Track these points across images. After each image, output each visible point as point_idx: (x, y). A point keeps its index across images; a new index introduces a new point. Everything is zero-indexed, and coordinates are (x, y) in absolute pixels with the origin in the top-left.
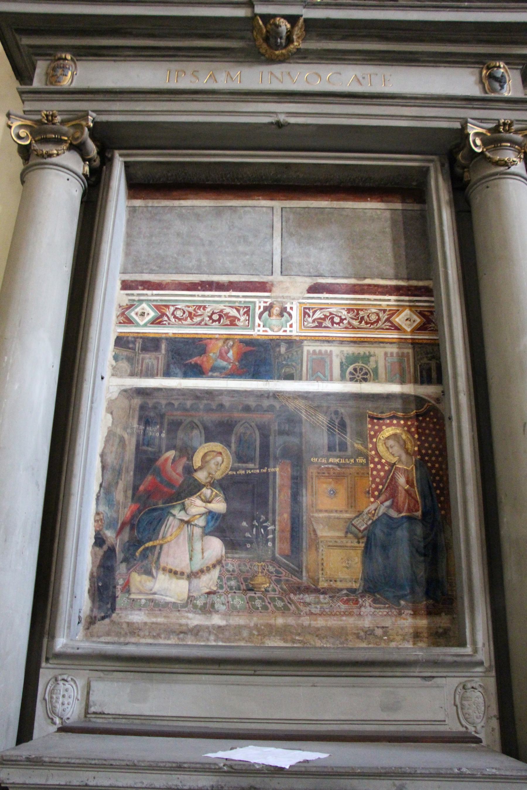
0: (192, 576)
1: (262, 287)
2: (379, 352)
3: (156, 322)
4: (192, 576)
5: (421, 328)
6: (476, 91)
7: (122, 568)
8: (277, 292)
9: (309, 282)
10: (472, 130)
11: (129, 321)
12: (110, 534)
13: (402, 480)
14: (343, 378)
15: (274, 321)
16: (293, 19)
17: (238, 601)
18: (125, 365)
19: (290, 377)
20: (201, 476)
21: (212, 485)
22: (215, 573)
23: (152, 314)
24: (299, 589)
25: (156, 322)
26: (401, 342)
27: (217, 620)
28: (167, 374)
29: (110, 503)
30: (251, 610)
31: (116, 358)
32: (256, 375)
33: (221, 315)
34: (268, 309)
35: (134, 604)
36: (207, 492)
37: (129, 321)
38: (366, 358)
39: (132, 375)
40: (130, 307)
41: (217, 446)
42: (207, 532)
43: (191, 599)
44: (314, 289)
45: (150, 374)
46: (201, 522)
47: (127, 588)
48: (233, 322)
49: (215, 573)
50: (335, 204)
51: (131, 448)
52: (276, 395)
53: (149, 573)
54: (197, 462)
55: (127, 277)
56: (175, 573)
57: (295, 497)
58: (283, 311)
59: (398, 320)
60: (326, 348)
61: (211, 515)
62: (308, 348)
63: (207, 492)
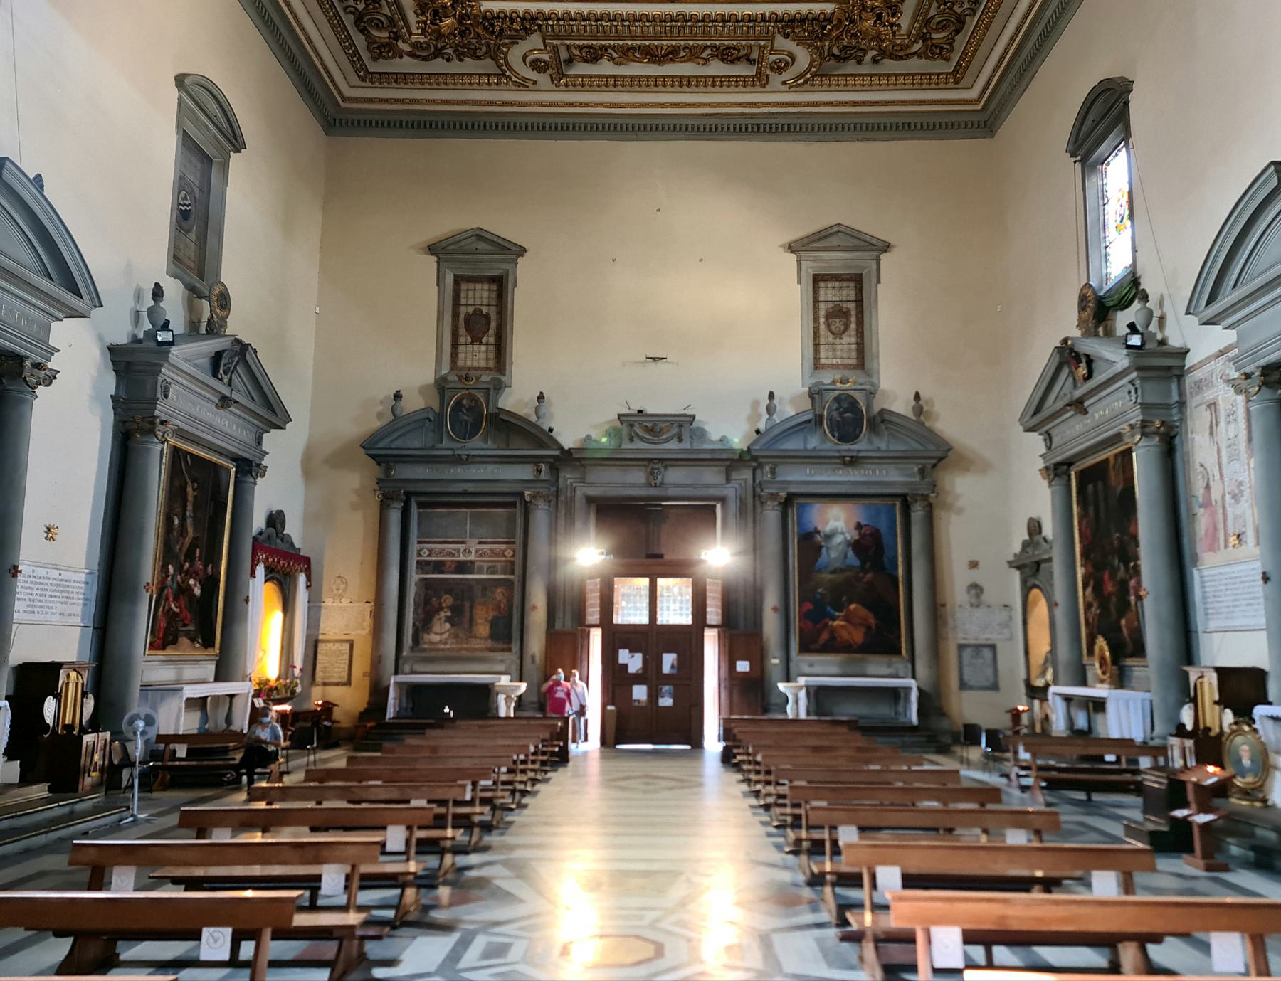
0: (441, 634)
1: (463, 543)
3: (429, 555)
4: (441, 634)
7: (421, 633)
8: (468, 545)
9: (477, 540)
11: (420, 555)
12: (417, 623)
13: (502, 606)
14: (487, 573)
15: (467, 554)
17: (454, 641)
18: (420, 571)
19: (470, 573)
21: (447, 607)
22: (447, 634)
23: (427, 553)
24: (471, 637)
25: (429, 555)
26: (505, 561)
27: (448, 646)
28: (433, 573)
29: (417, 614)
30: (457, 643)
31: (417, 568)
32: (460, 573)
33: (450, 553)
34: (465, 550)
35: (425, 643)
36: (445, 610)
37: (420, 555)
38: (494, 567)
39: (422, 573)
41: (447, 596)
42: (446, 621)
43: (441, 641)
44: (480, 543)
45: (427, 573)
46: (444, 619)
47: (422, 639)
48: (453, 555)
49: (447, 634)
51: (423, 597)
52: (467, 579)
53: (428, 633)
54: (442, 601)
55: (419, 539)
56: (436, 634)
57: (471, 611)
58: (469, 551)
59: (506, 553)
60: (482, 564)
61: (446, 617)
62: (477, 564)
63: (445, 610)
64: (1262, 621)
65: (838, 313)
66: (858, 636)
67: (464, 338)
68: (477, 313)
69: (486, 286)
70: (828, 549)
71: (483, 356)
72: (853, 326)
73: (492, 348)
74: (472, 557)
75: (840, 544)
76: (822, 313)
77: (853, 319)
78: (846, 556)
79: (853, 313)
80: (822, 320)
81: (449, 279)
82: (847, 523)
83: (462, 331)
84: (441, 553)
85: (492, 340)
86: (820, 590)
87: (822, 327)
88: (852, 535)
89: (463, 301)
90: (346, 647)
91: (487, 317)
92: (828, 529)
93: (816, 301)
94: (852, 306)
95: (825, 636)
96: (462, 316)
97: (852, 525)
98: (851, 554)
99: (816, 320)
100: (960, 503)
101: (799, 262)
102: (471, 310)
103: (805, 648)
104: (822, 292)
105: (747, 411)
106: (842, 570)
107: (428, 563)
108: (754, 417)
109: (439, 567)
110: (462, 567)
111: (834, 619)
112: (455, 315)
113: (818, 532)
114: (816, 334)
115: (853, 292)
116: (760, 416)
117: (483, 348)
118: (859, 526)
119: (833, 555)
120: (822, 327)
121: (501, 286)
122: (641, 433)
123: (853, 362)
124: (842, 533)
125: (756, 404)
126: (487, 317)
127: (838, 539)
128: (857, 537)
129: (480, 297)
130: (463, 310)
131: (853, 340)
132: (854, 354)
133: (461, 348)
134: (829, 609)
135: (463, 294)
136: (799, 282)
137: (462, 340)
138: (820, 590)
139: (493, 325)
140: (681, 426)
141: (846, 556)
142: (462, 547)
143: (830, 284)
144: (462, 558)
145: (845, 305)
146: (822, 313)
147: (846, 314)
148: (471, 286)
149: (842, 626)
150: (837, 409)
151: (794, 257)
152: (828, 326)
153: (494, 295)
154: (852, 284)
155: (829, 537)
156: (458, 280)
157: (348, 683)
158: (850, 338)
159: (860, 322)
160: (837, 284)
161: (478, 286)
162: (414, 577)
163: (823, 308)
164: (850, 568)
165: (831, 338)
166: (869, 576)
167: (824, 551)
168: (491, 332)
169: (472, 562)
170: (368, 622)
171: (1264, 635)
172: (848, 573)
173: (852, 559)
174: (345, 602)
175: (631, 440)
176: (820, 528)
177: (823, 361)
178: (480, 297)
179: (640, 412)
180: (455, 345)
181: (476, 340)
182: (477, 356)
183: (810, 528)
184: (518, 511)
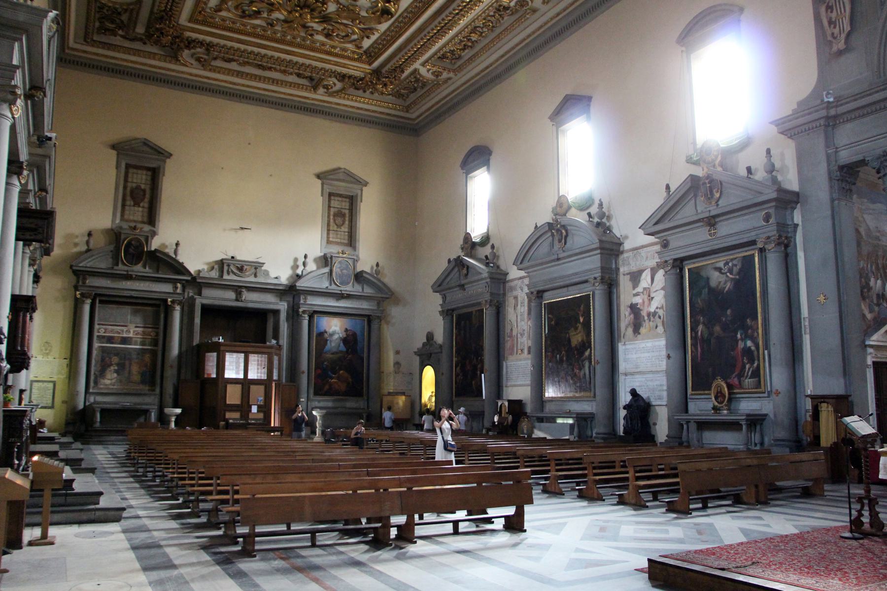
0: (111, 380)
1: (126, 326)
2: (147, 340)
3: (104, 333)
5: (156, 336)
6: (172, 291)
7: (99, 378)
9: (135, 325)
10: (169, 300)
11: (99, 332)
12: (96, 372)
16: (136, 275)
20: (113, 363)
21: (115, 364)
23: (104, 331)
26: (151, 339)
28: (107, 343)
34: (127, 331)
35: (101, 384)
39: (100, 343)
40: (99, 329)
41: (116, 357)
45: (104, 343)
48: (119, 333)
49: (115, 379)
50: (143, 308)
52: (127, 348)
53: (103, 379)
56: (109, 379)
57: (130, 367)
59: (152, 334)
61: (115, 369)
62: (134, 339)
64: (529, 382)
65: (339, 214)
66: (343, 387)
67: (129, 202)
68: (138, 187)
69: (145, 172)
70: (331, 341)
71: (140, 214)
72: (347, 222)
73: (146, 210)
74: (131, 335)
75: (337, 339)
76: (332, 213)
77: (347, 219)
78: (339, 346)
79: (347, 215)
80: (332, 217)
81: (123, 166)
82: (340, 328)
83: (128, 198)
84: (112, 331)
85: (146, 205)
86: (325, 363)
87: (332, 221)
88: (342, 335)
89: (130, 180)
90: (51, 385)
91: (144, 191)
92: (331, 331)
93: (329, 207)
94: (347, 212)
95: (327, 387)
96: (129, 189)
97: (343, 330)
98: (342, 344)
99: (329, 217)
100: (394, 321)
101: (323, 184)
102: (134, 185)
103: (316, 393)
104: (332, 202)
105: (292, 263)
106: (336, 353)
107: (104, 337)
108: (295, 267)
109: (110, 340)
110: (125, 341)
111: (332, 378)
112: (125, 188)
113: (326, 332)
114: (328, 225)
115: (348, 204)
116: (297, 267)
117: (140, 209)
118: (346, 330)
119: (333, 345)
120: (332, 221)
121: (155, 175)
122: (235, 271)
123: (346, 241)
124: (338, 334)
125: (296, 260)
126: (144, 191)
127: (336, 336)
128: (345, 336)
129: (141, 179)
130: (129, 185)
131: (346, 230)
132: (347, 237)
133: (127, 208)
134: (330, 373)
135: (130, 175)
136: (322, 195)
137: (128, 203)
138: (325, 363)
139: (148, 196)
140: (256, 268)
141: (339, 346)
142: (125, 329)
143: (336, 198)
144: (125, 335)
145: (343, 211)
146: (332, 213)
147: (344, 215)
148: (135, 171)
149: (335, 382)
150: (339, 268)
151: (319, 182)
152: (335, 221)
153: (149, 178)
154: (348, 200)
155: (331, 335)
156: (128, 166)
157: (52, 407)
158: (345, 228)
159: (351, 221)
160: (340, 199)
161: (140, 172)
162: (96, 345)
163: (332, 210)
164: (341, 352)
165: (335, 228)
166: (350, 356)
167: (328, 342)
168: (146, 200)
169: (131, 338)
170: (65, 370)
171: (530, 387)
172: (340, 355)
173: (342, 348)
174: (50, 358)
175: (228, 273)
176: (327, 330)
177: (331, 239)
178: (141, 179)
179: (233, 257)
180: (123, 206)
181: (137, 204)
182: (138, 213)
183: (322, 330)
184: (162, 309)
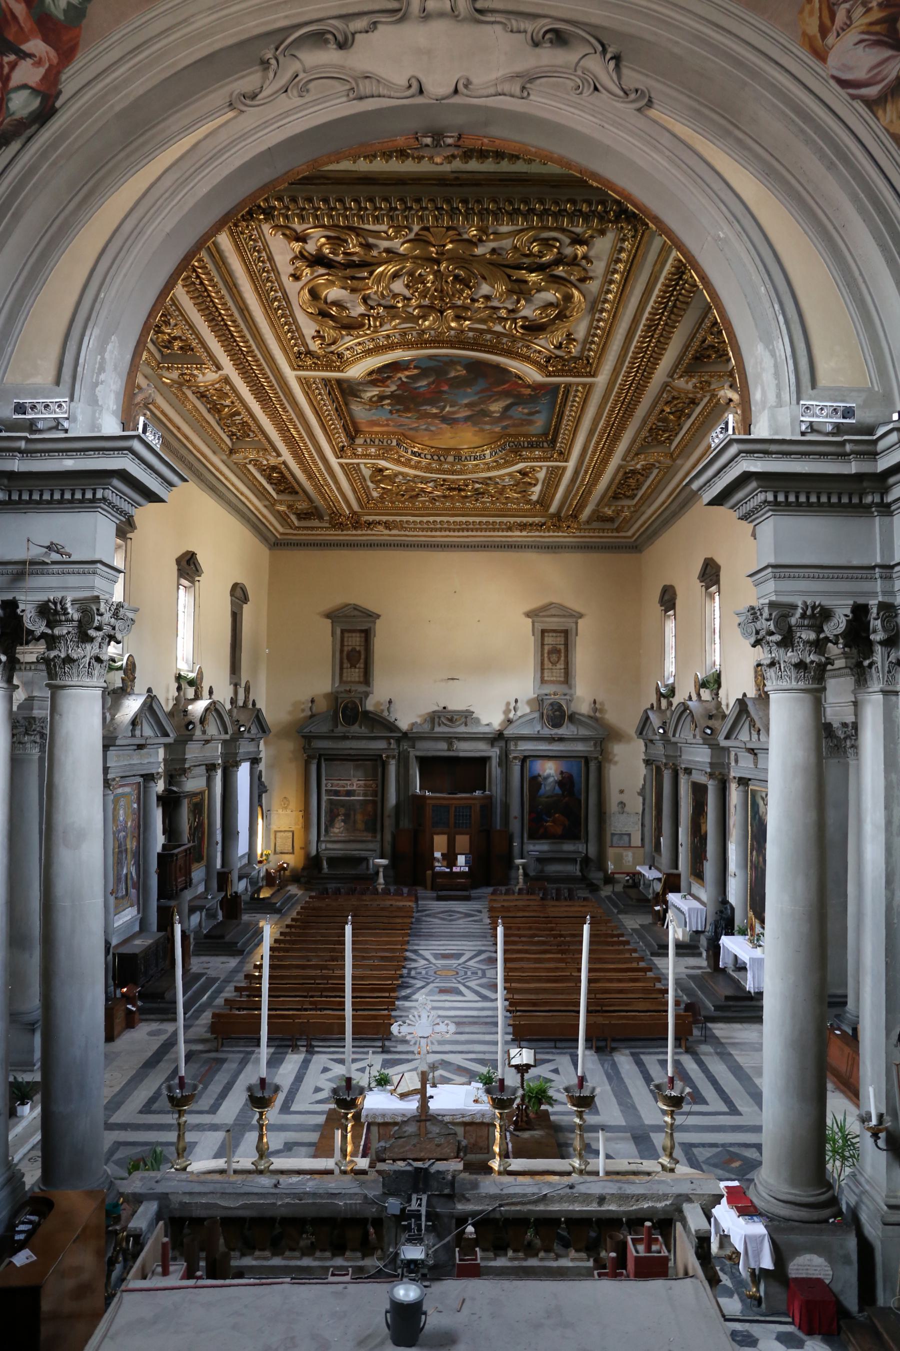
65: (554, 651)
67: (346, 664)
68: (353, 650)
69: (358, 635)
71: (357, 675)
72: (562, 658)
73: (362, 670)
76: (546, 651)
77: (563, 655)
79: (563, 651)
80: (546, 655)
81: (338, 632)
82: (556, 771)
83: (345, 661)
85: (362, 666)
87: (546, 659)
88: (558, 777)
89: (346, 644)
91: (359, 652)
92: (545, 774)
93: (543, 645)
94: (562, 647)
96: (345, 653)
97: (559, 772)
98: (557, 787)
99: (542, 655)
101: (533, 623)
102: (350, 648)
104: (546, 639)
105: (503, 708)
106: (552, 797)
111: (547, 822)
112: (342, 651)
114: (542, 664)
115: (563, 639)
116: (510, 711)
117: (357, 670)
118: (562, 773)
119: (547, 788)
120: (546, 659)
121: (367, 635)
122: (445, 722)
123: (562, 679)
125: (508, 704)
126: (359, 652)
127: (551, 779)
129: (355, 641)
130: (346, 649)
131: (562, 667)
132: (562, 675)
133: (345, 671)
134: (544, 817)
135: (346, 639)
136: (533, 635)
137: (345, 666)
139: (363, 657)
140: (466, 717)
143: (551, 634)
145: (558, 647)
146: (546, 651)
147: (559, 651)
148: (350, 635)
151: (530, 620)
152: (549, 659)
153: (363, 639)
154: (563, 635)
155: (546, 778)
158: (561, 665)
159: (566, 656)
160: (554, 634)
161: (354, 635)
163: (546, 648)
164: (557, 795)
165: (550, 666)
166: (567, 799)
168: (362, 661)
173: (558, 790)
175: (439, 725)
176: (541, 773)
177: (546, 678)
178: (355, 641)
179: (444, 708)
180: (341, 669)
181: (353, 666)
183: (536, 773)
